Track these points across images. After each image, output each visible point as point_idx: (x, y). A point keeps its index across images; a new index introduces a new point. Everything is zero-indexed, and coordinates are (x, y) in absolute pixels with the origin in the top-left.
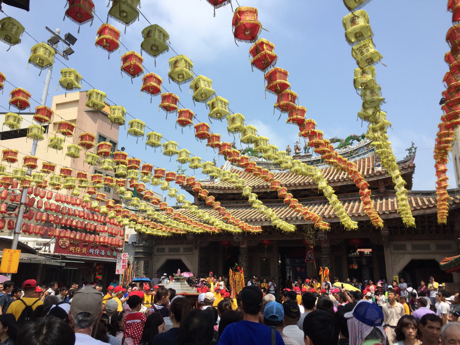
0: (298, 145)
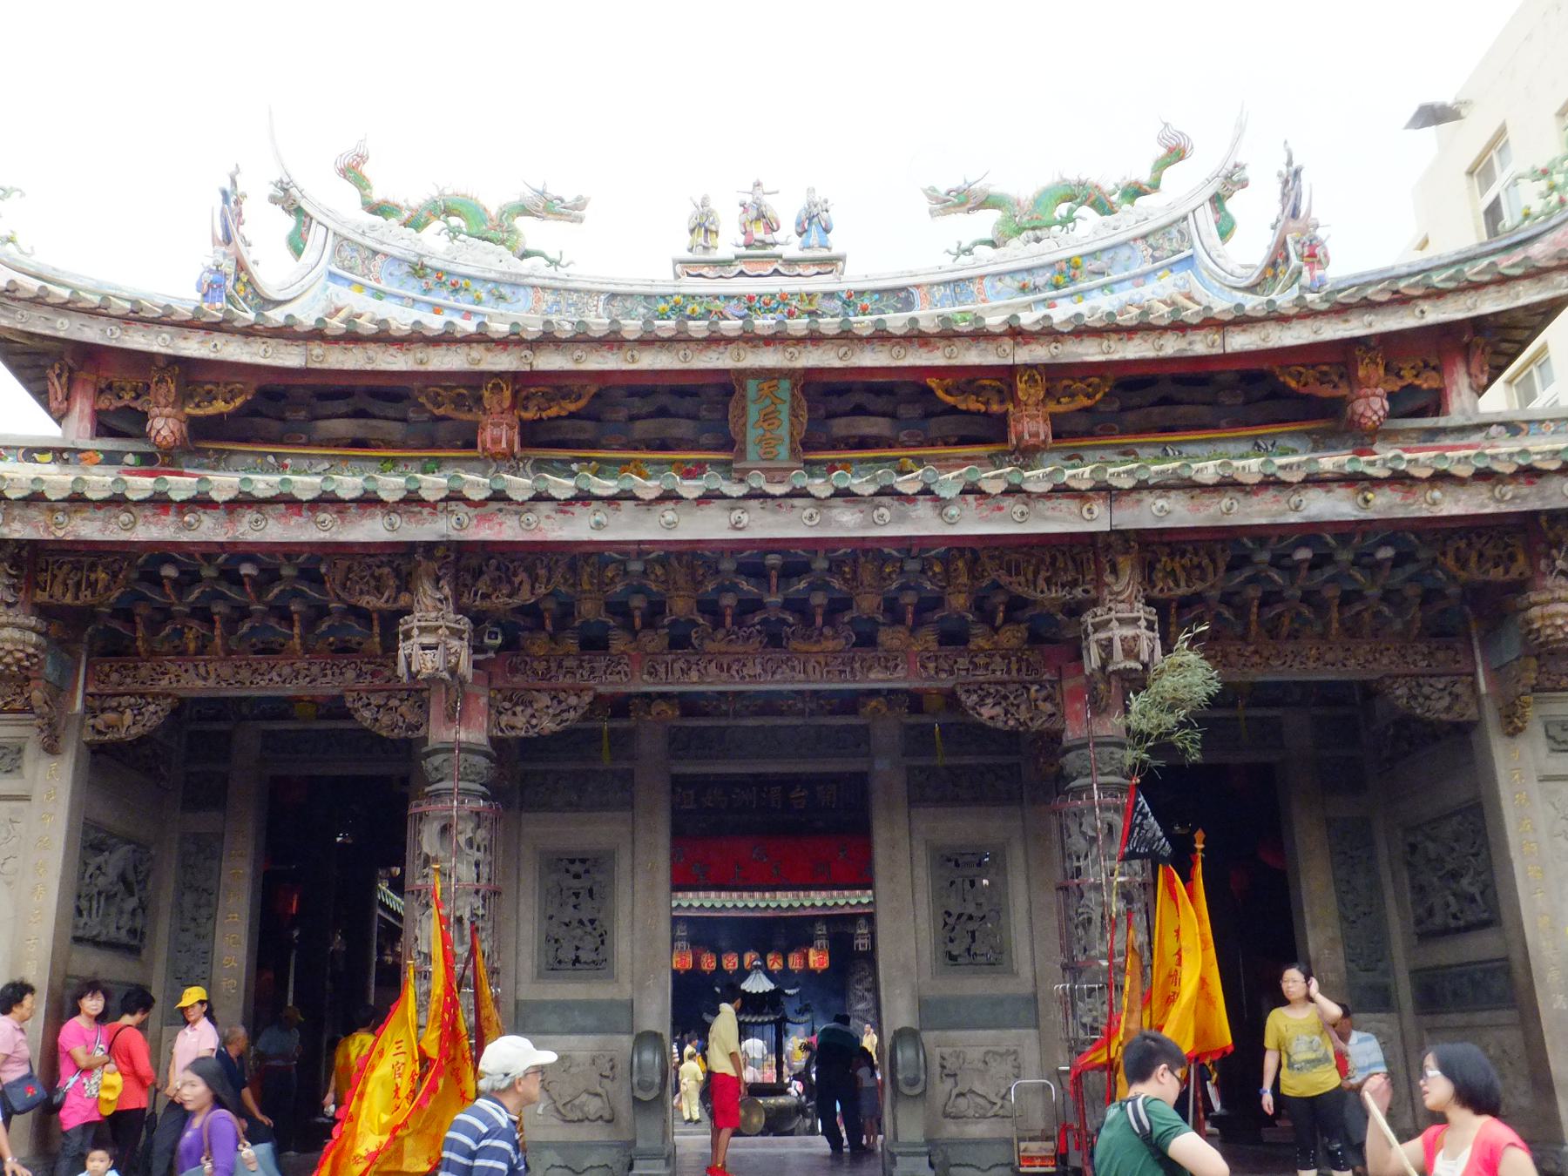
0: (767, 199)
